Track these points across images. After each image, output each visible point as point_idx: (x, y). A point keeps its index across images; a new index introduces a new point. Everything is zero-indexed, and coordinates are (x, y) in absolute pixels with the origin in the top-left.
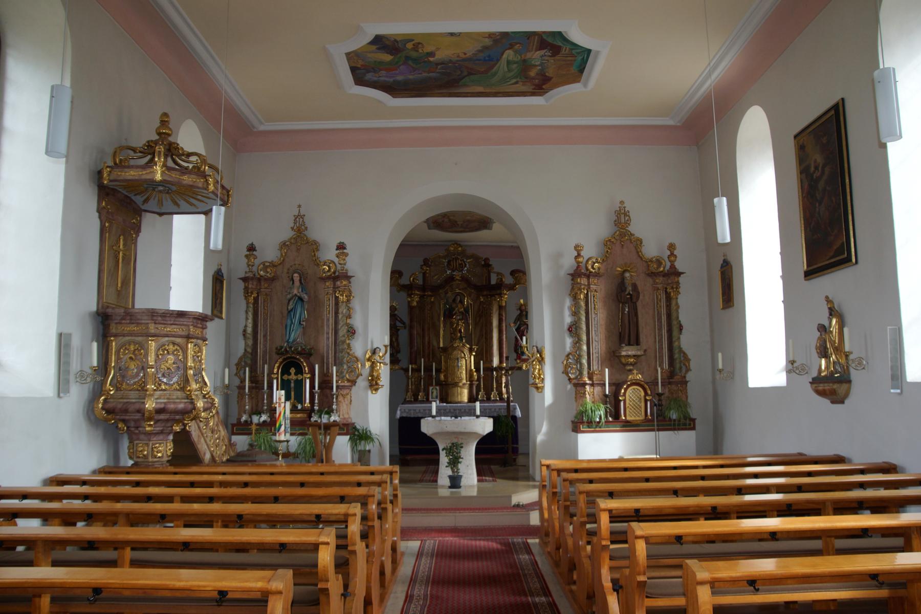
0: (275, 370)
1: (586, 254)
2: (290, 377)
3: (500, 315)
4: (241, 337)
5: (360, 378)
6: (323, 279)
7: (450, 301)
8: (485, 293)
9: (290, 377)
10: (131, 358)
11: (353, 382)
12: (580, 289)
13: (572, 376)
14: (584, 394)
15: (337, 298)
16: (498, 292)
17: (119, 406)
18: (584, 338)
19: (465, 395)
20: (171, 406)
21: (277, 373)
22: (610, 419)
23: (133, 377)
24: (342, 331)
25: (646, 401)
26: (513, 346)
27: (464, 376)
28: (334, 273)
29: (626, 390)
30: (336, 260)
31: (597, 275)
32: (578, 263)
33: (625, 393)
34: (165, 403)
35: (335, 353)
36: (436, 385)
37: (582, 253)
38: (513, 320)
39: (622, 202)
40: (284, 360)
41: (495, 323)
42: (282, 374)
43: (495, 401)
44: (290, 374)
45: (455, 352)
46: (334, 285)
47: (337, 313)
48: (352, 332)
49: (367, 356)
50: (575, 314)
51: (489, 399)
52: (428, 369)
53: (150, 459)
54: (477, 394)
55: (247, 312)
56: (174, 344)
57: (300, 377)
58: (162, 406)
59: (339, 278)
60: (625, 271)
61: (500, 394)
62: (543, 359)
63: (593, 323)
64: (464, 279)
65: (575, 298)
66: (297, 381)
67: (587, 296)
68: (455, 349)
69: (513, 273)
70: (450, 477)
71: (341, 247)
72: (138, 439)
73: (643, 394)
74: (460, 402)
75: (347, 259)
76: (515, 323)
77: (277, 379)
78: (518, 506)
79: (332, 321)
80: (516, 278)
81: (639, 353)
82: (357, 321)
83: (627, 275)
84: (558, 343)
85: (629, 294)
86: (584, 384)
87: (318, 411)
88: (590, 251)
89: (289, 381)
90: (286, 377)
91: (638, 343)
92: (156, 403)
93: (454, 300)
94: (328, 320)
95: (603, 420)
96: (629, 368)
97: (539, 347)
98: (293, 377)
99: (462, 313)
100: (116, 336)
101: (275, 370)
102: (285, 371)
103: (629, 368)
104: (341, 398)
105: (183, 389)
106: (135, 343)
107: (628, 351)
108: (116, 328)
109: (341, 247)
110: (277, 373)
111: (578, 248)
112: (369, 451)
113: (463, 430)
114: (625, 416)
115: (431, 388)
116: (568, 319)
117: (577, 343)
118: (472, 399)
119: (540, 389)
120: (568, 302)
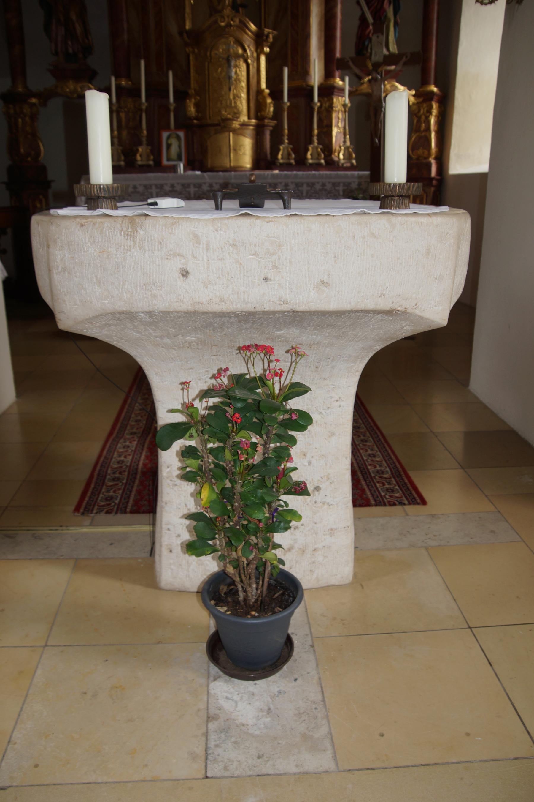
19: (243, 151)
27: (243, 106)
36: (178, 127)
43: (317, 166)
51: (301, 163)
52: (157, 90)
54: (275, 150)
61: (328, 149)
68: (221, 33)
74: (235, 169)
115: (165, 135)
118: (262, 161)
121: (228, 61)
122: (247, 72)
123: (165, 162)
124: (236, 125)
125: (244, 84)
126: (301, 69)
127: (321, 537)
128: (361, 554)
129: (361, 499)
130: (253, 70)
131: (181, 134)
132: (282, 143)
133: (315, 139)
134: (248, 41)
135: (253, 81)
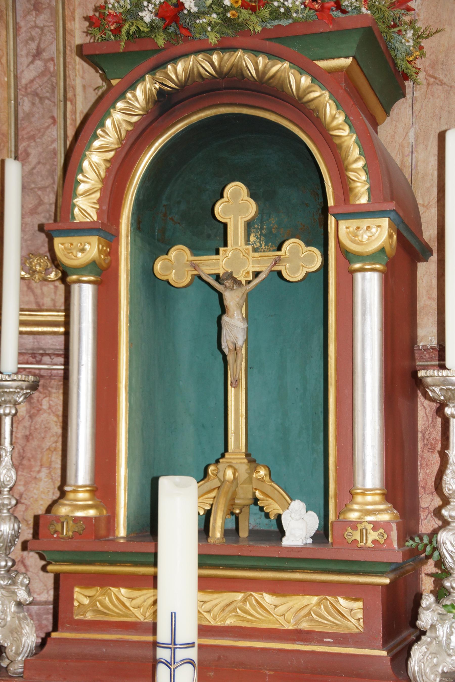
0: (86, 207)
21: (105, 229)
40: (165, 104)
44: (212, 236)
57: (299, 259)
77: (104, 276)
90: (176, 265)
98: (240, 258)
101: (86, 207)
102: (174, 207)
110: (105, 229)
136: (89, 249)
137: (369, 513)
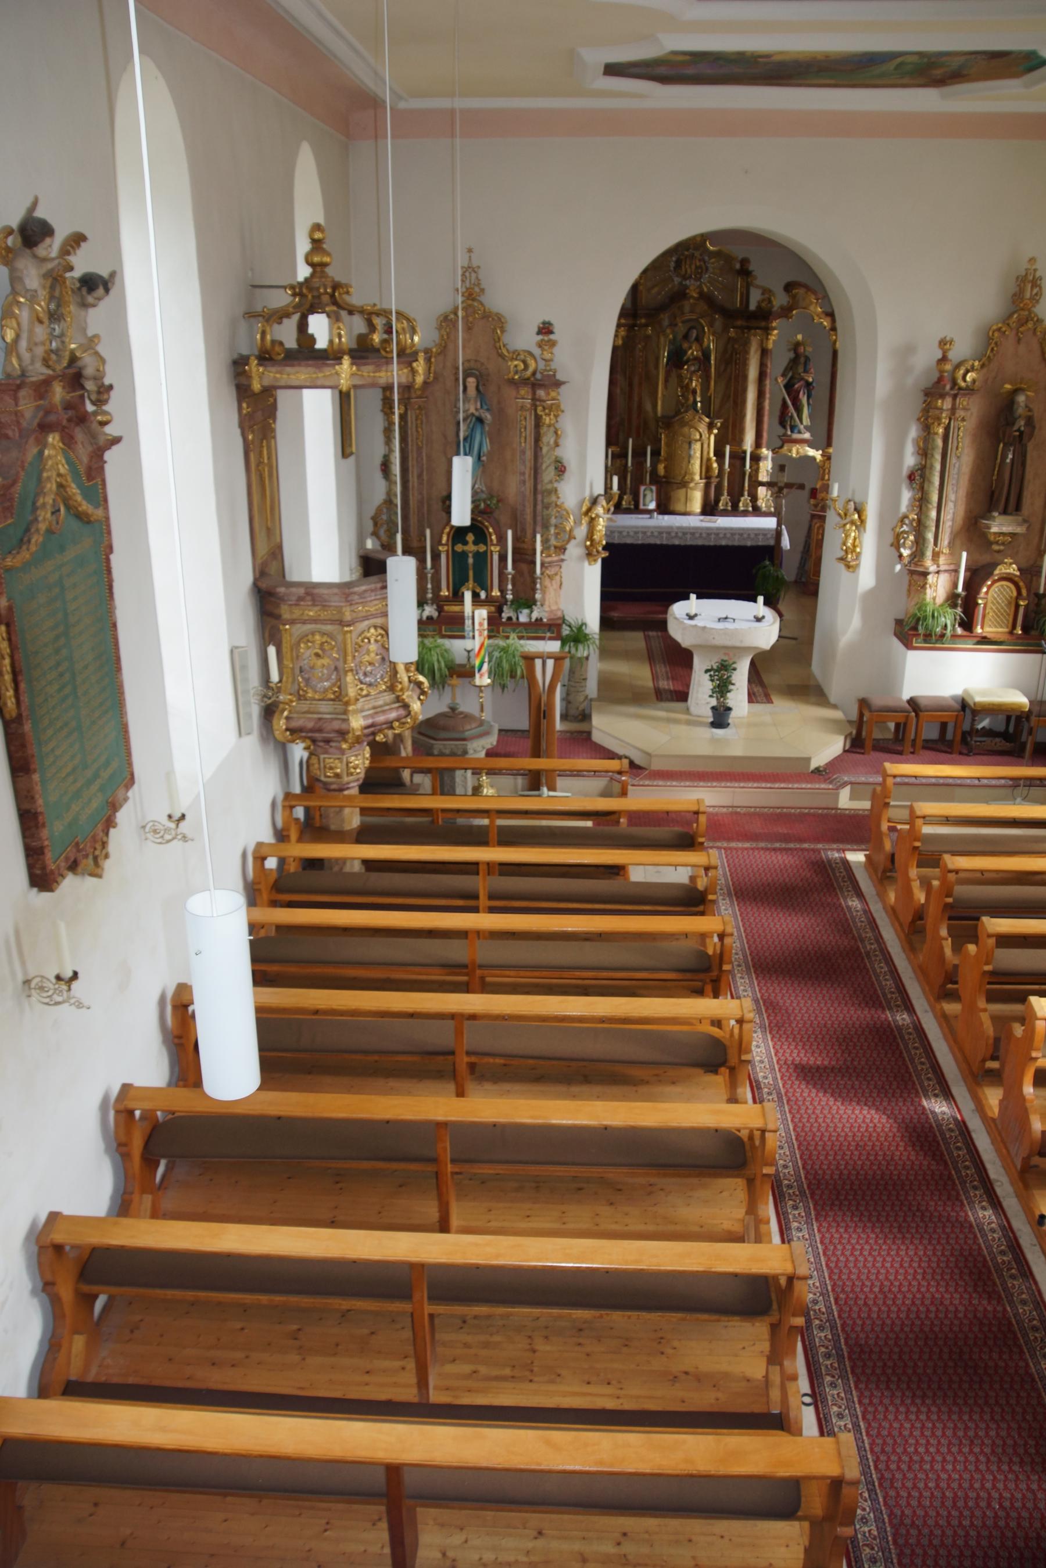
0: (444, 540)
1: (956, 353)
2: (466, 548)
3: (762, 366)
4: (378, 475)
5: (573, 542)
6: (512, 382)
7: (680, 336)
8: (739, 323)
9: (466, 548)
10: (317, 655)
11: (562, 549)
12: (939, 419)
13: (906, 552)
14: (924, 587)
15: (538, 420)
16: (763, 324)
17: (310, 725)
18: (935, 498)
20: (381, 718)
22: (959, 631)
23: (321, 680)
24: (548, 474)
25: (1017, 606)
26: (777, 413)
28: (534, 373)
29: (989, 587)
30: (537, 352)
31: (970, 390)
32: (941, 372)
33: (987, 593)
34: (371, 716)
35: (535, 511)
36: (651, 483)
37: (951, 355)
38: (781, 369)
39: (1032, 260)
41: (753, 373)
42: (453, 545)
43: (745, 514)
44: (466, 543)
45: (686, 429)
46: (534, 393)
47: (537, 439)
48: (561, 469)
49: (584, 509)
50: (924, 452)
52: (639, 454)
53: (346, 779)
54: (717, 501)
55: (388, 431)
56: (375, 627)
57: (482, 548)
58: (370, 721)
59: (543, 384)
60: (1016, 391)
62: (862, 521)
63: (952, 472)
64: (702, 296)
65: (927, 429)
66: (477, 555)
67: (947, 429)
68: (684, 424)
69: (789, 287)
70: (713, 708)
71: (546, 329)
72: (326, 753)
73: (1015, 594)
75: (556, 350)
76: (784, 375)
78: (817, 770)
79: (529, 454)
80: (794, 297)
81: (1019, 530)
82: (568, 451)
83: (1021, 399)
84: (889, 498)
85: (1019, 430)
86: (925, 574)
87: (512, 602)
88: (963, 349)
89: (464, 555)
90: (459, 548)
91: (1018, 508)
92: (365, 717)
93: (686, 337)
94: (523, 452)
95: (949, 632)
96: (996, 547)
97: (857, 500)
99: (696, 358)
100: (292, 622)
101: (444, 540)
103: (996, 547)
104: (547, 582)
105: (391, 688)
106: (323, 634)
107: (999, 525)
108: (291, 613)
109: (546, 329)
110: (447, 544)
111: (944, 343)
112: (587, 658)
113: (738, 644)
114: (982, 628)
115: (642, 488)
116: (910, 460)
117: (921, 502)
119: (851, 567)
120: (914, 432)
121: (690, 443)
122: (700, 446)
123: (641, 507)
124: (692, 485)
125: (698, 454)
126: (739, 440)
127: (738, 697)
128: (749, 712)
129: (749, 702)
130: (705, 446)
131: (654, 488)
132: (722, 495)
133: (746, 493)
134: (703, 428)
135: (705, 453)
136: (446, 548)
137: (496, 593)
